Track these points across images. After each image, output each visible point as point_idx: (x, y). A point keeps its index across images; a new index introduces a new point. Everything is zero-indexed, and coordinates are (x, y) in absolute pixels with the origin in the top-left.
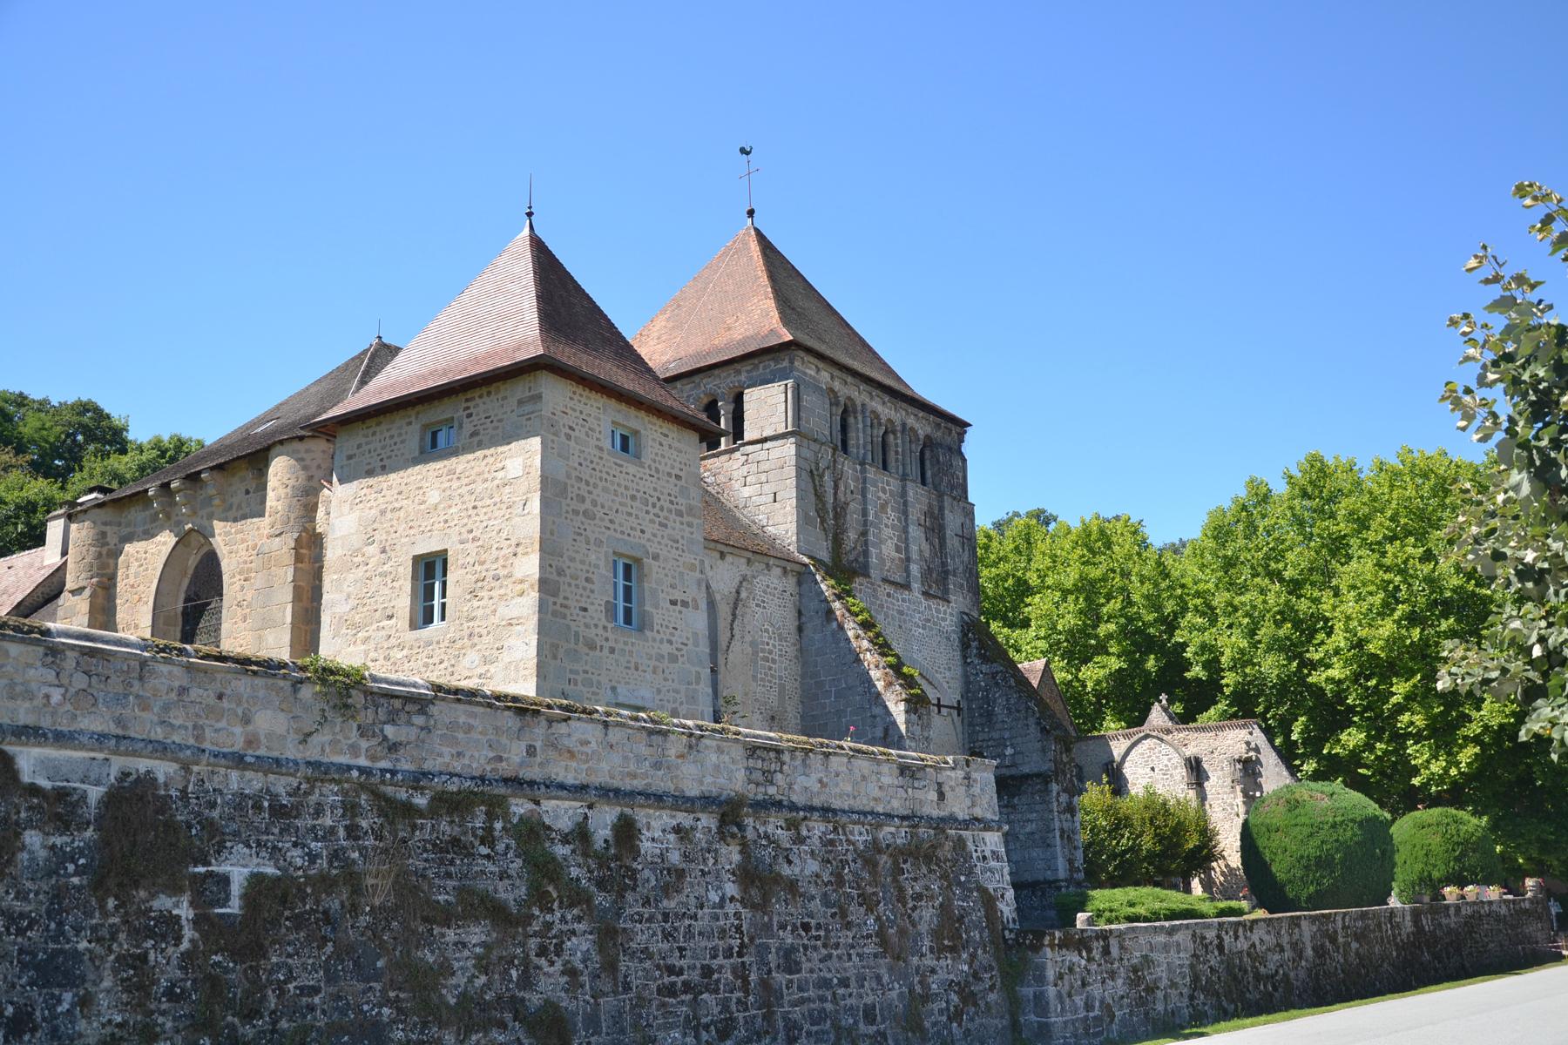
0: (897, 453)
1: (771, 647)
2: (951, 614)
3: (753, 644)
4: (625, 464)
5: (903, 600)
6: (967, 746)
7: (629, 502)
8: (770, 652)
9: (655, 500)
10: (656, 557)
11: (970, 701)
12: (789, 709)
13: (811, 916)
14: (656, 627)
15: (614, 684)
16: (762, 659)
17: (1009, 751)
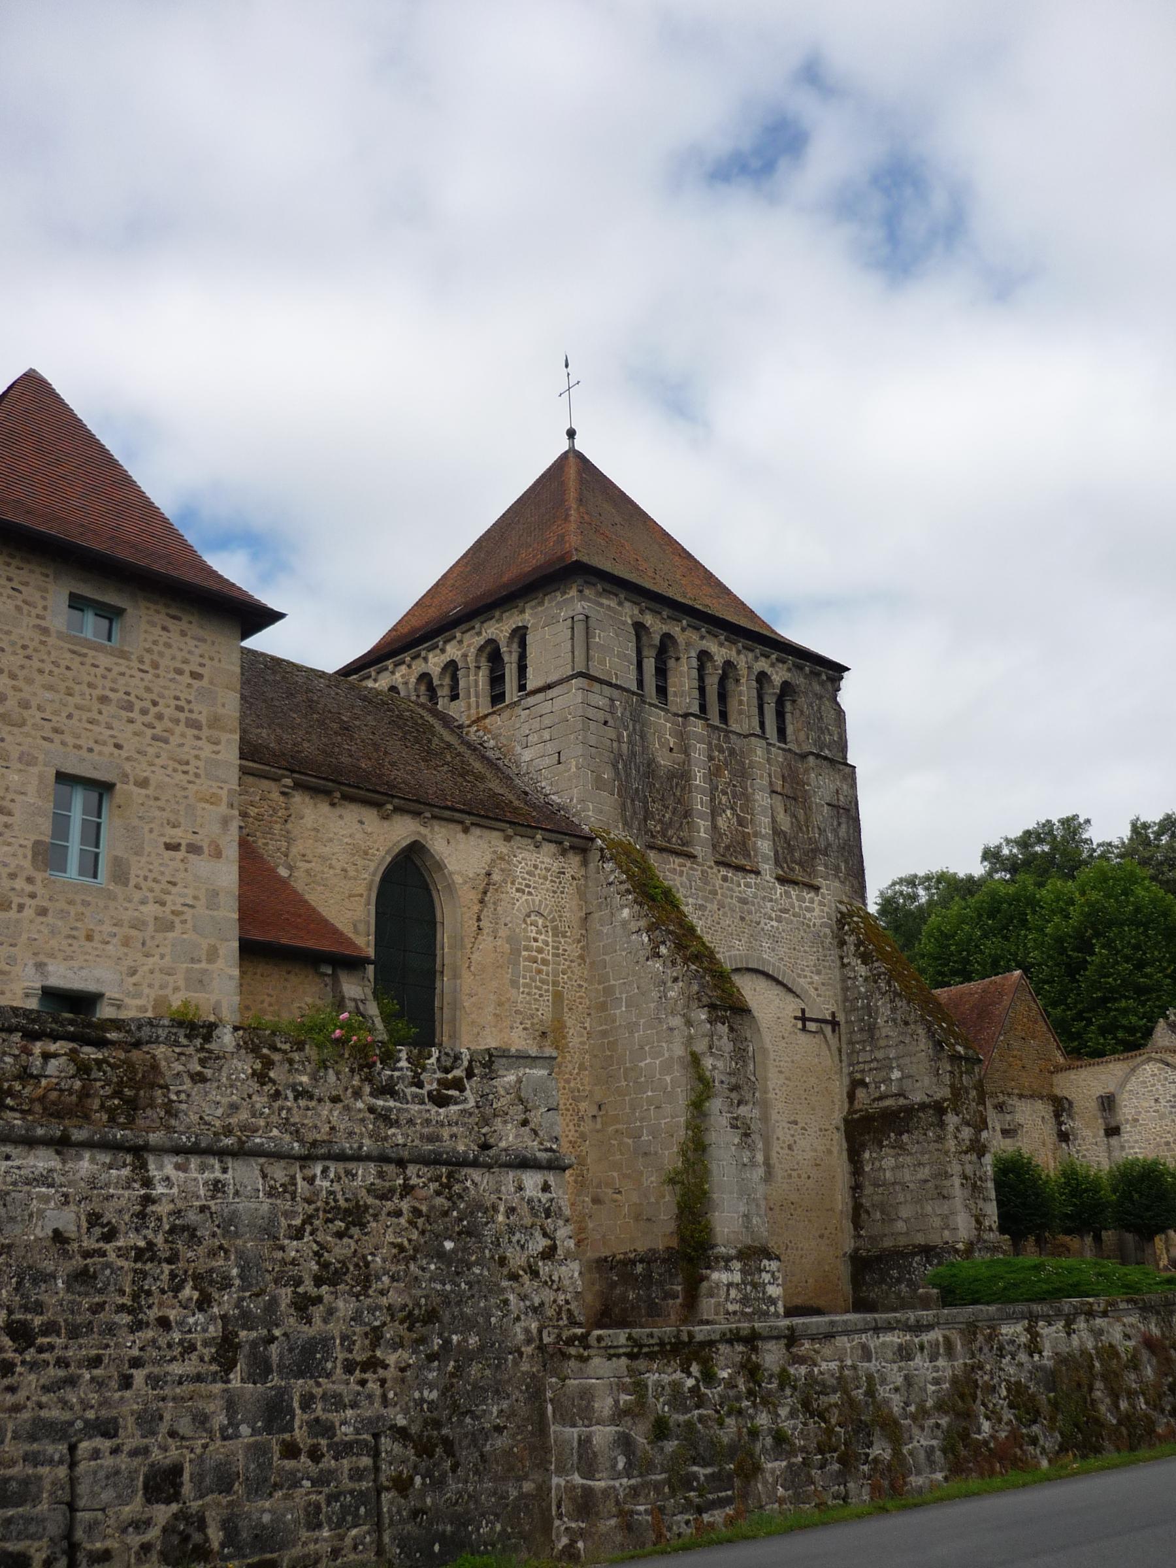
0: (741, 702)
1: (540, 944)
2: (821, 904)
4: (91, 653)
5: (748, 885)
6: (845, 1071)
7: (96, 706)
8: (540, 951)
9: (148, 704)
10: (144, 783)
11: (847, 1012)
12: (569, 1023)
14: (132, 883)
15: (42, 958)
16: (526, 959)
17: (896, 1074)
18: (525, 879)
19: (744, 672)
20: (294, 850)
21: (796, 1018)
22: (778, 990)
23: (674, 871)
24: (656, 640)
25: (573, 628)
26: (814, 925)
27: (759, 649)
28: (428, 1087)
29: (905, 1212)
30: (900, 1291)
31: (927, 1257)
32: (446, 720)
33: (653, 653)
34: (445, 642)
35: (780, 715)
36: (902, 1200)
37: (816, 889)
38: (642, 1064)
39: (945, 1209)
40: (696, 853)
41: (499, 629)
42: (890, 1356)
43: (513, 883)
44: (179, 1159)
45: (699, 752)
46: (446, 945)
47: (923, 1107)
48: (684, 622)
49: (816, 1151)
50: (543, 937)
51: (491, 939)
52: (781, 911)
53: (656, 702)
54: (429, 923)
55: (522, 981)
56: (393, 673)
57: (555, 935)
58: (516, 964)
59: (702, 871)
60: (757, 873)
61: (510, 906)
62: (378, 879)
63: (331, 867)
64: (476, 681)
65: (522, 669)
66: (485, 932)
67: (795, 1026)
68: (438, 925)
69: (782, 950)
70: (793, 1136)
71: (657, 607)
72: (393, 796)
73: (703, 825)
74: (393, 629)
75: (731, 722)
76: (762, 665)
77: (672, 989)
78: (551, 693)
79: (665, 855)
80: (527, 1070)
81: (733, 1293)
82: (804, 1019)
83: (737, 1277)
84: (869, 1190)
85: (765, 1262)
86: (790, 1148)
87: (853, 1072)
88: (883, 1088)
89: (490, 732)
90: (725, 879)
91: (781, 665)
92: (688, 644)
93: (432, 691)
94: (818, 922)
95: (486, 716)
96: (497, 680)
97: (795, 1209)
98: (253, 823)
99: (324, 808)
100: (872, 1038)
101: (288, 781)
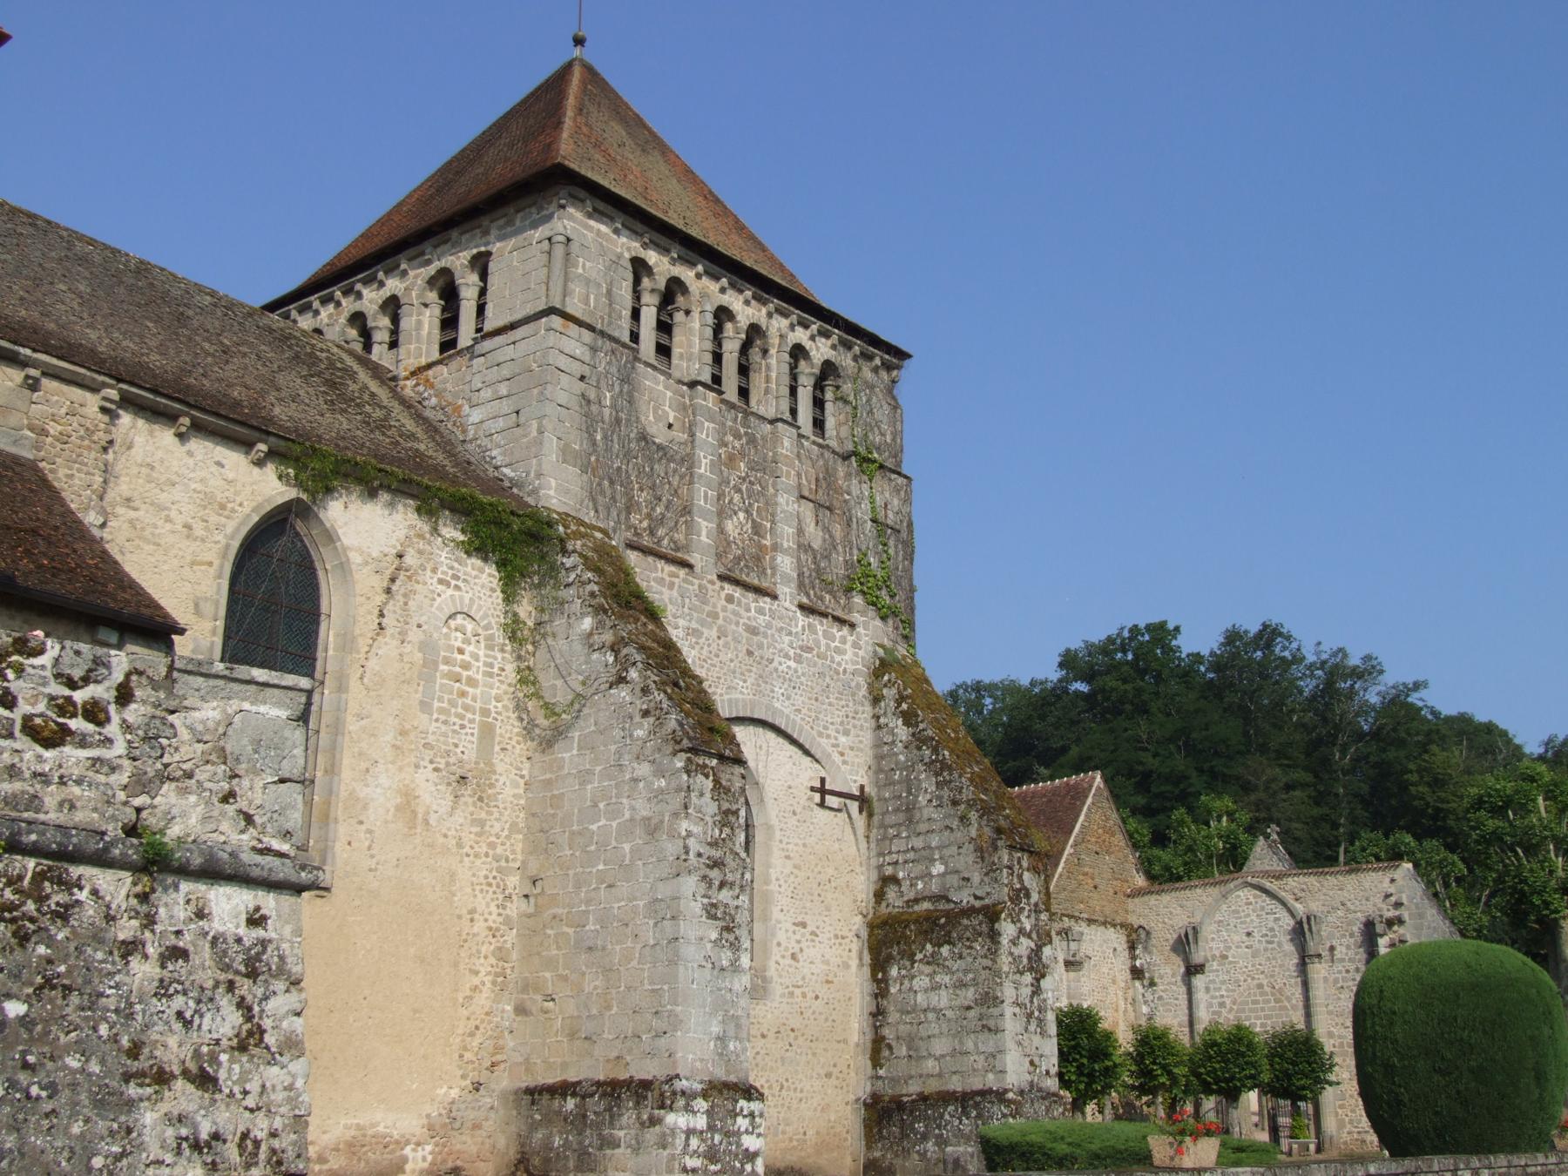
1: (466, 657)
2: (856, 645)
5: (761, 611)
6: (874, 862)
8: (466, 666)
12: (500, 768)
17: (938, 869)
18: (452, 568)
19: (774, 340)
21: (813, 789)
23: (661, 581)
24: (661, 284)
26: (845, 671)
28: (24, 708)
29: (940, 1046)
30: (926, 1152)
31: (964, 1108)
32: (377, 371)
36: (936, 1031)
37: (852, 626)
38: (594, 827)
39: (988, 1043)
40: (692, 561)
43: (434, 570)
45: (706, 432)
46: (331, 646)
47: (969, 912)
49: (827, 963)
50: (470, 649)
51: (396, 643)
52: (801, 648)
53: (655, 363)
55: (436, 704)
57: (490, 647)
58: (430, 680)
59: (700, 586)
60: (775, 597)
61: (427, 601)
62: (236, 544)
63: (168, 520)
64: (423, 322)
65: (481, 310)
66: (389, 631)
67: (810, 799)
69: (799, 699)
70: (798, 942)
72: (268, 433)
73: (705, 529)
75: (753, 402)
76: (801, 336)
77: (641, 726)
79: (650, 559)
80: (246, 706)
82: (823, 791)
83: (701, 1122)
84: (893, 1017)
85: (742, 1103)
86: (793, 956)
87: (882, 865)
88: (920, 885)
89: (432, 386)
90: (730, 599)
91: (823, 340)
94: (850, 668)
95: (429, 366)
96: (450, 322)
97: (796, 1038)
98: (52, 445)
99: (165, 436)
100: (911, 821)
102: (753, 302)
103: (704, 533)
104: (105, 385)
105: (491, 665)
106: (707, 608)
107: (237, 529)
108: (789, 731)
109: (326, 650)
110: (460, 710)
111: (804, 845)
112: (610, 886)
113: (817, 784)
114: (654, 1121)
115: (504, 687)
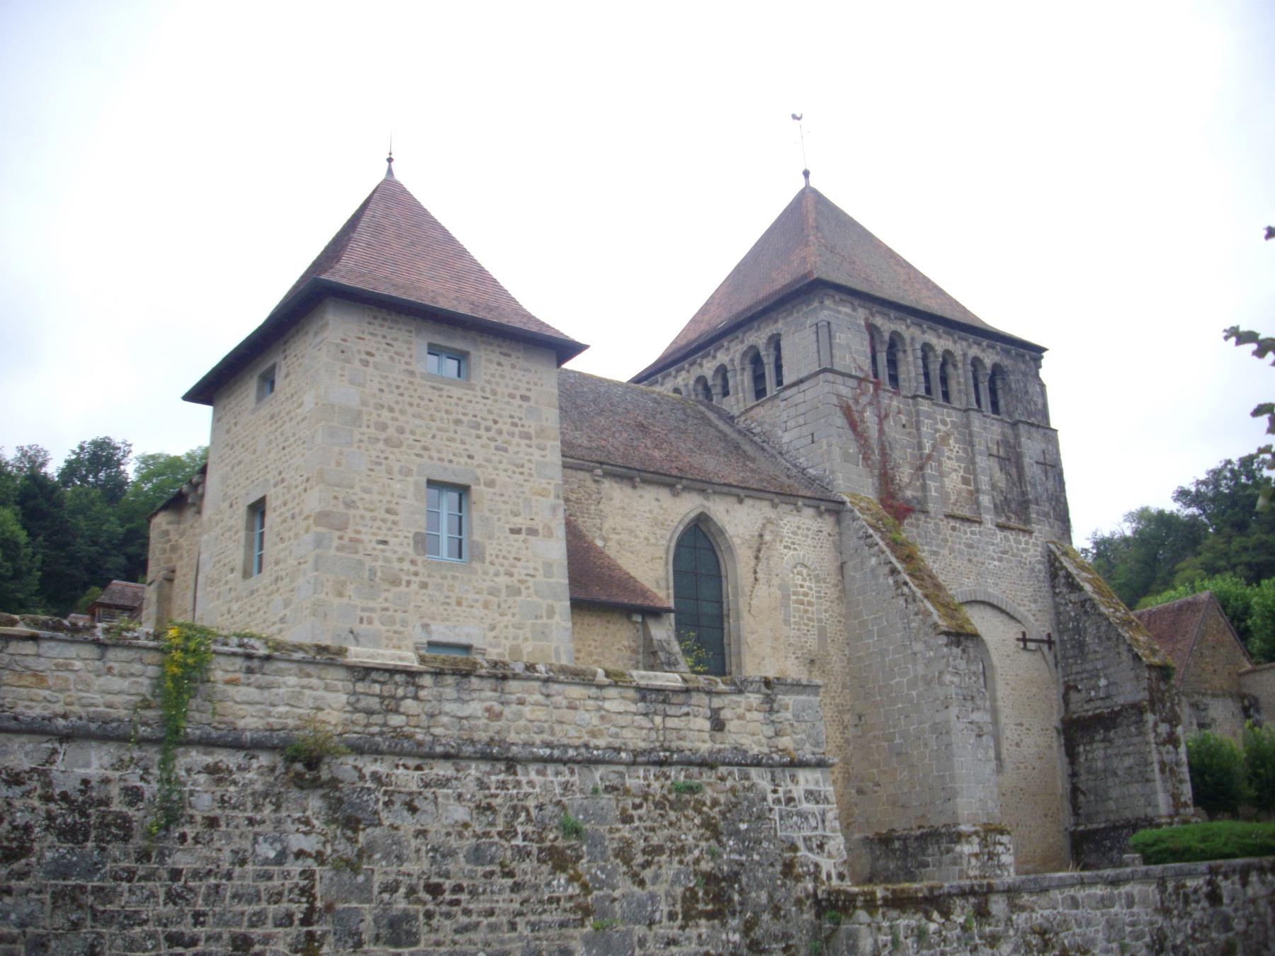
0: (959, 383)
1: (805, 589)
2: (1035, 545)
3: (783, 587)
4: (447, 387)
5: (973, 533)
6: (1061, 681)
7: (452, 427)
8: (806, 595)
9: (490, 423)
10: (491, 484)
11: (1061, 633)
12: (832, 652)
13: (447, 875)
14: (488, 559)
15: (426, 620)
16: (797, 602)
17: (1103, 682)
18: (790, 538)
19: (959, 358)
20: (606, 526)
21: (1018, 639)
22: (1003, 617)
24: (887, 336)
25: (817, 333)
27: (971, 338)
29: (1114, 793)
32: (719, 412)
33: (885, 347)
34: (716, 350)
35: (993, 391)
37: (1031, 533)
38: (893, 682)
41: (758, 337)
42: (1094, 904)
43: (781, 541)
44: (540, 766)
46: (730, 594)
48: (909, 321)
49: (1038, 746)
50: (807, 584)
51: (766, 587)
54: (717, 577)
55: (792, 620)
56: (675, 377)
57: (817, 582)
58: (786, 606)
62: (673, 544)
63: (636, 537)
64: (742, 381)
65: (779, 368)
67: (1017, 646)
68: (723, 579)
70: (1019, 735)
71: (885, 310)
74: (674, 342)
76: (974, 351)
77: (914, 620)
78: (802, 387)
81: (973, 861)
82: (1024, 640)
83: (976, 849)
86: (1017, 745)
88: (1093, 693)
90: (954, 529)
91: (991, 350)
92: (913, 339)
93: (707, 390)
94: (1033, 560)
95: (752, 408)
96: (759, 378)
99: (629, 490)
101: (599, 471)
102: (944, 336)
103: (933, 489)
104: (595, 468)
105: (820, 592)
106: (941, 537)
107: (672, 537)
108: (1000, 605)
109: (728, 597)
110: (806, 621)
111: (1017, 675)
112: (906, 717)
113: (1020, 636)
114: (948, 851)
115: (828, 604)
